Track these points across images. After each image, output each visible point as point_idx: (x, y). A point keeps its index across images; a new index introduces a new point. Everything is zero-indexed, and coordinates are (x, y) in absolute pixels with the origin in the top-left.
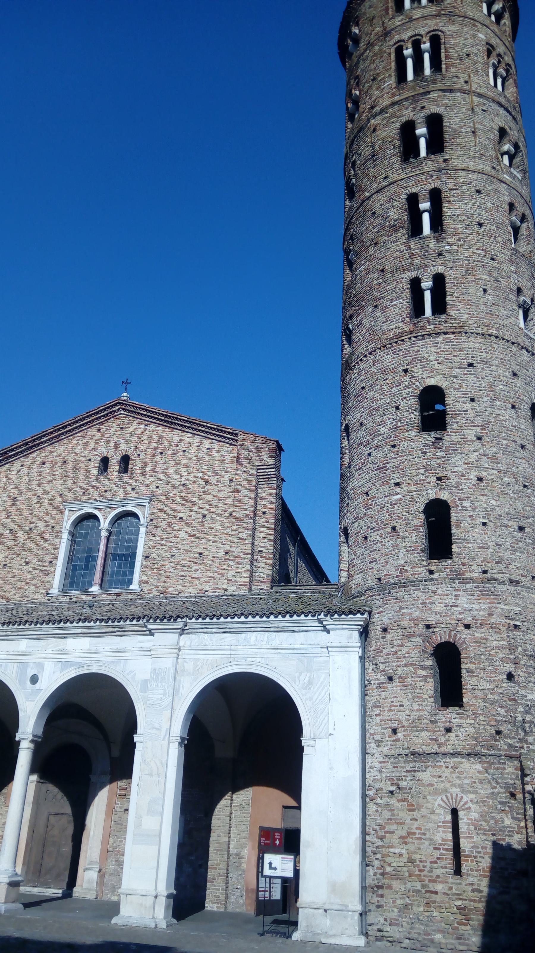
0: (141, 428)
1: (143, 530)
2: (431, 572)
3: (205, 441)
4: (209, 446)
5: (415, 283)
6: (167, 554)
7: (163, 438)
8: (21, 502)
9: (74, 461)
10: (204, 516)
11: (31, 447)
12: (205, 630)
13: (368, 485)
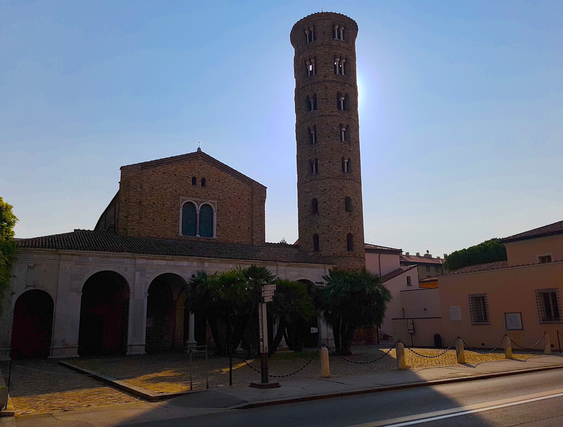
1: (215, 214)
5: (343, 159)
8: (156, 190)
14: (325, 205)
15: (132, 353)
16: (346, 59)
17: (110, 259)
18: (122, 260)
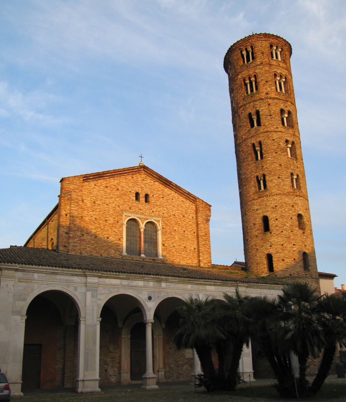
0: (152, 182)
1: (160, 232)
2: (306, 275)
3: (180, 197)
4: (182, 200)
5: (292, 174)
6: (172, 245)
7: (163, 190)
8: (99, 205)
9: (122, 190)
10: (184, 231)
11: (100, 177)
12: (253, 287)
13: (282, 242)
14: (277, 222)
15: (86, 390)
16: (286, 78)
17: (58, 277)
18: (71, 278)
